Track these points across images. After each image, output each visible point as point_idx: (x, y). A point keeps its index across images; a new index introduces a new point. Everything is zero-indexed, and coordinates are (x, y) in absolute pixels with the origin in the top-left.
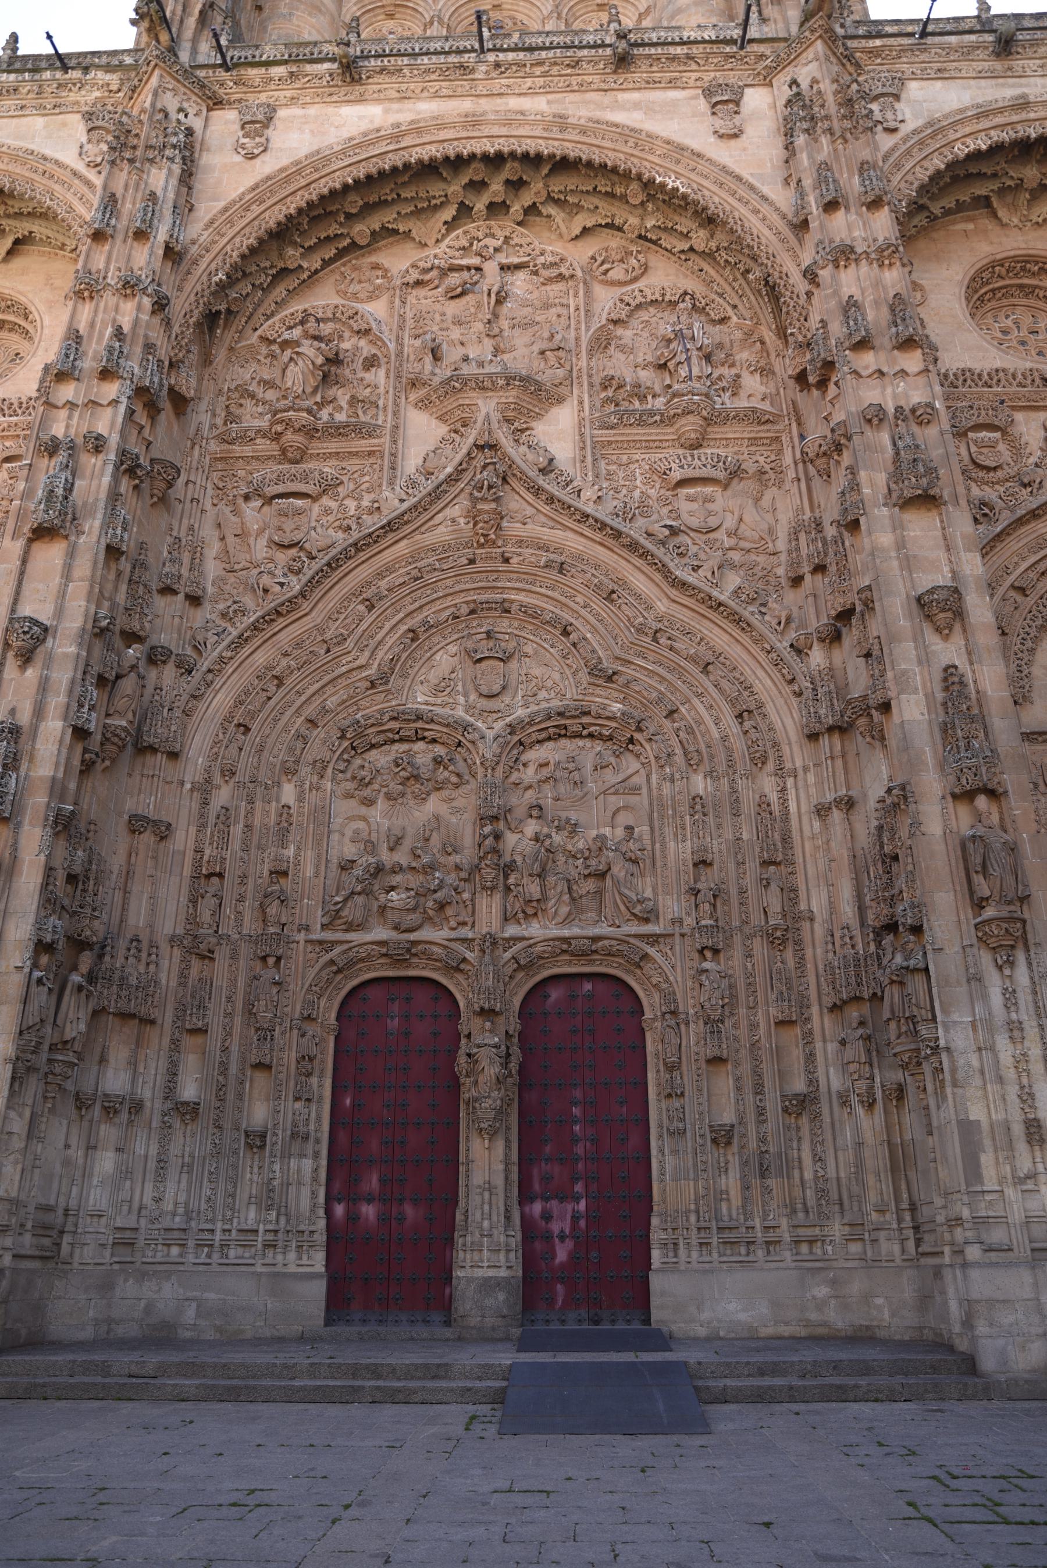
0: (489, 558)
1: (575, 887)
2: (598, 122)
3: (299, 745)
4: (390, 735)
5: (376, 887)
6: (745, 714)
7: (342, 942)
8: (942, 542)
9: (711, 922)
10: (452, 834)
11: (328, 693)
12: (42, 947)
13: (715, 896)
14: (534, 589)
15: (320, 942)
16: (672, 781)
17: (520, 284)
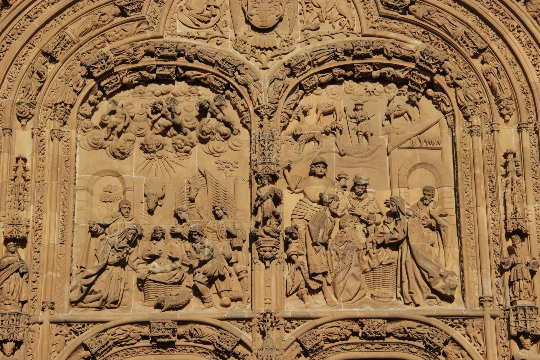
3: (35, 84)
4: (145, 73)
7: (95, 323)
10: (221, 193)
11: (67, 19)
15: (69, 323)
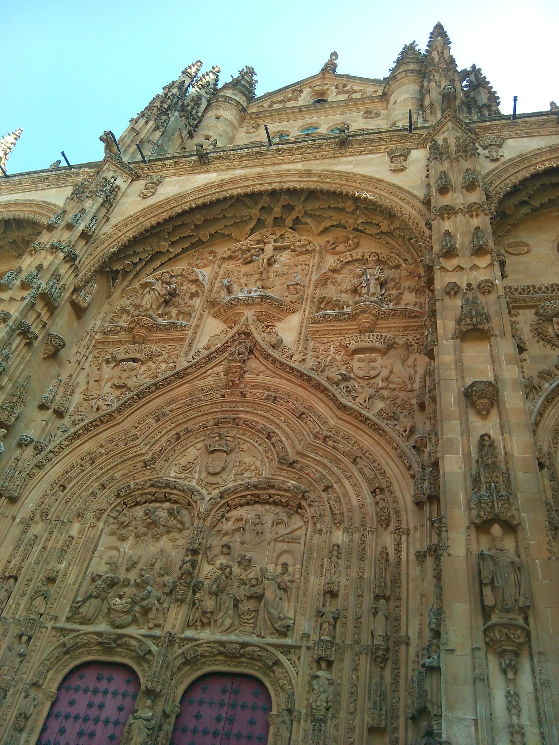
0: (232, 394)
1: (241, 606)
3: (91, 498)
4: (149, 497)
5: (110, 595)
6: (378, 490)
8: (489, 359)
9: (328, 638)
13: (335, 619)
14: (255, 411)
15: (61, 630)
16: (321, 534)
17: (284, 257)
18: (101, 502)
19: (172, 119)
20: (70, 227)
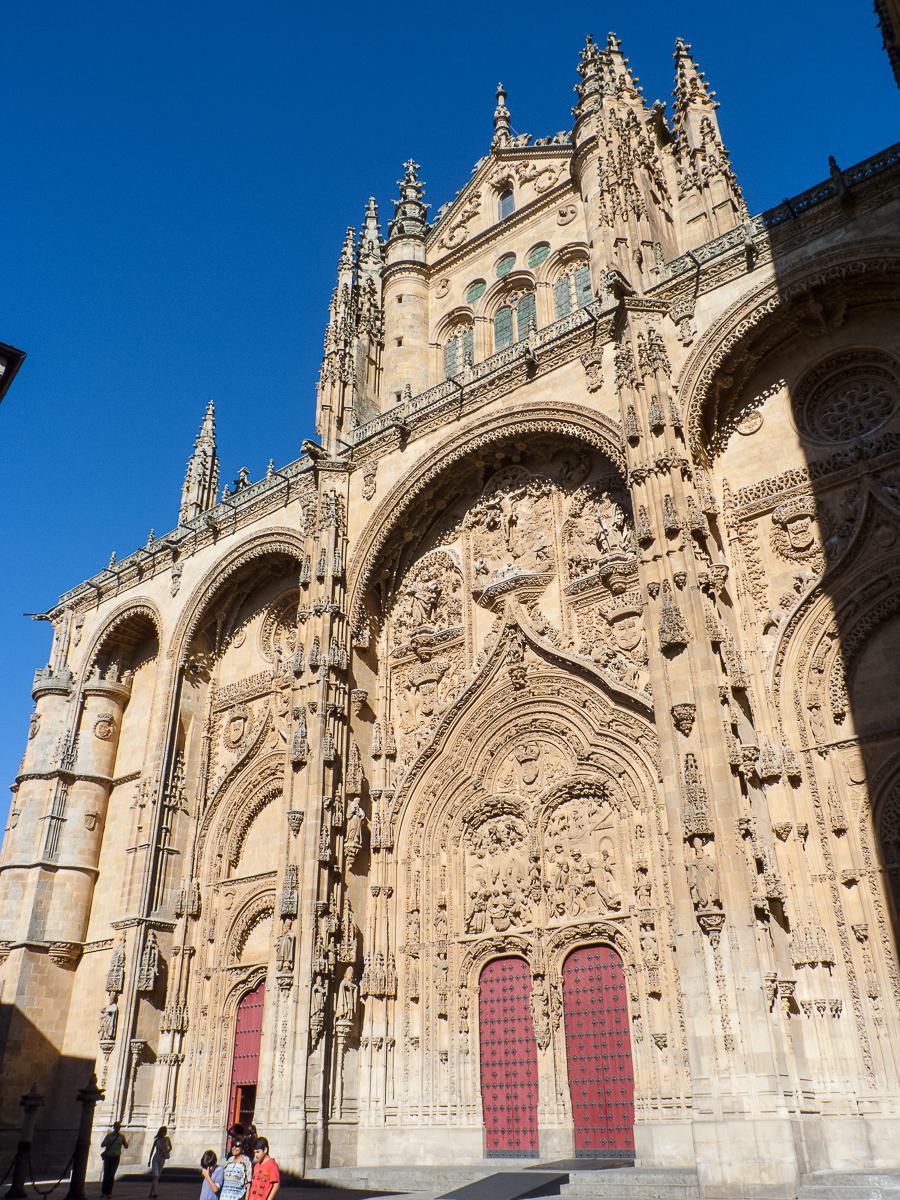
2: (528, 405)
3: (445, 829)
12: (316, 974)
17: (524, 507)
18: (454, 831)
19: (354, 352)
20: (321, 579)
